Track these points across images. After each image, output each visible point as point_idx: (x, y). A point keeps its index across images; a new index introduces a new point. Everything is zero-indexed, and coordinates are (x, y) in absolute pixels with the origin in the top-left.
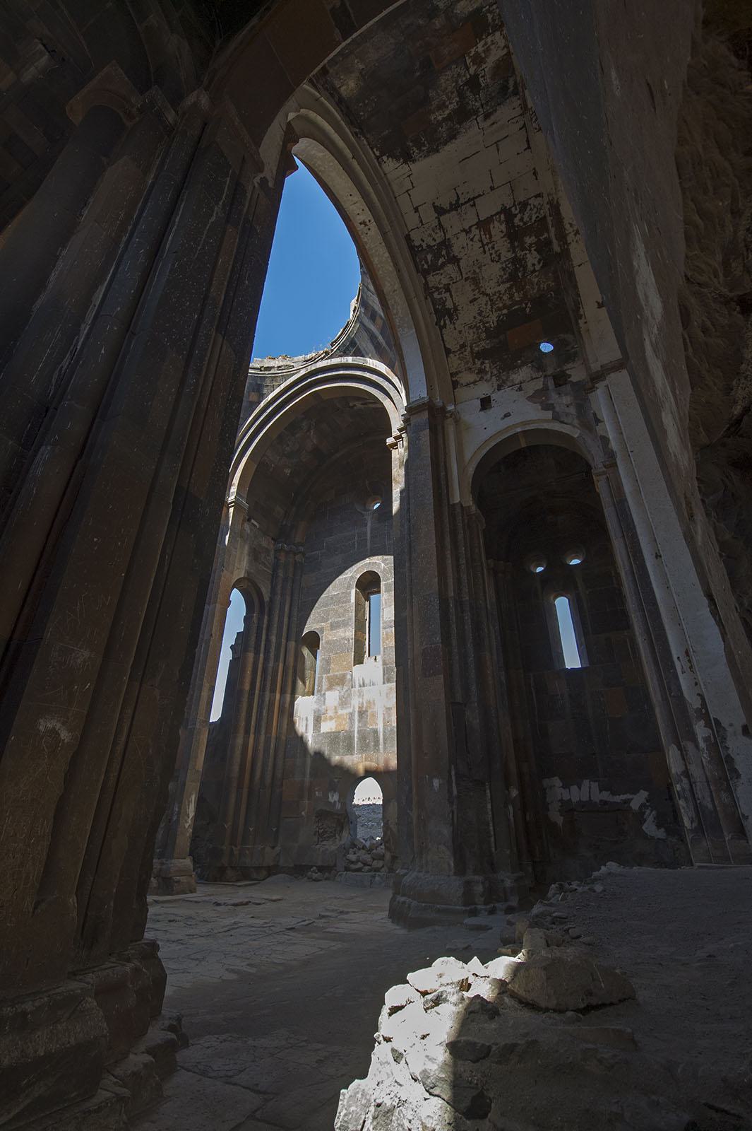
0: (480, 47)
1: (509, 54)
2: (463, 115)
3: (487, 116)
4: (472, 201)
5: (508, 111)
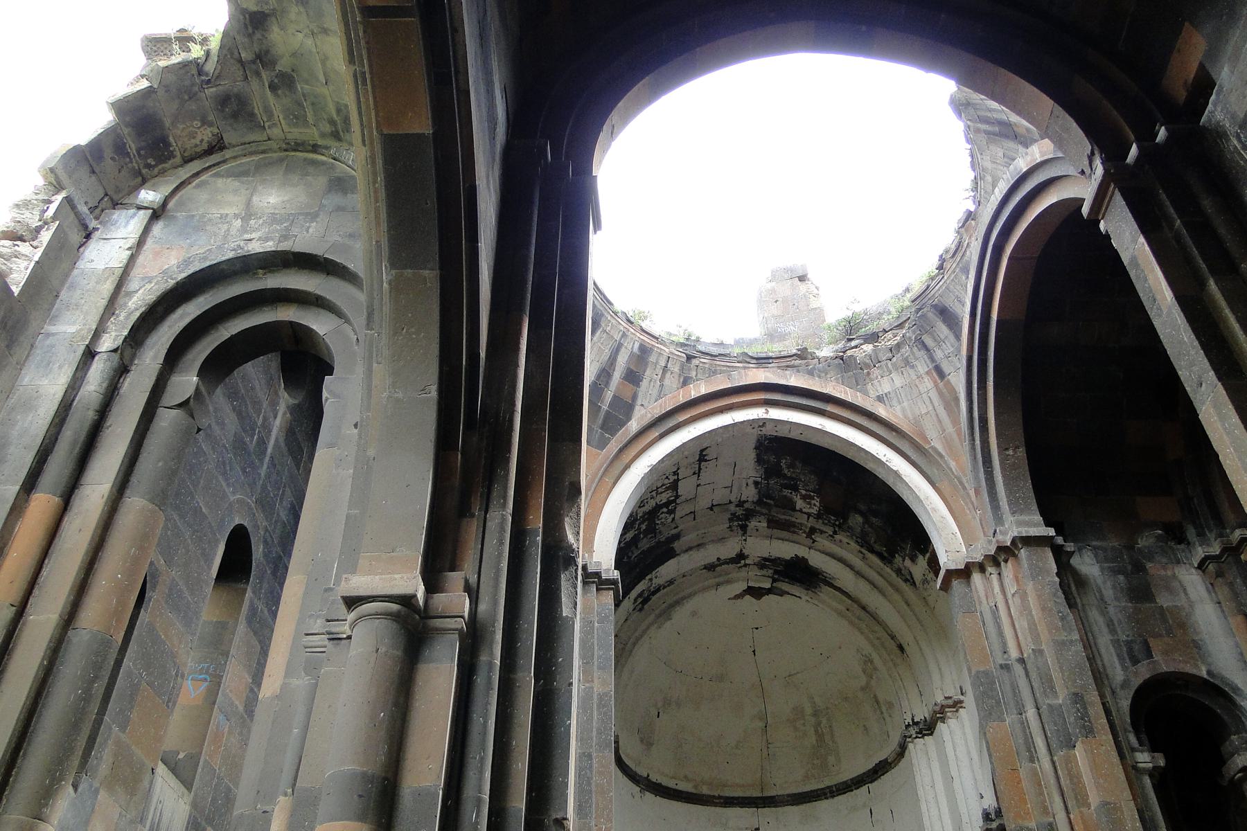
0: (816, 502)
1: (794, 509)
2: (771, 471)
3: (756, 483)
4: (698, 473)
5: (750, 494)
